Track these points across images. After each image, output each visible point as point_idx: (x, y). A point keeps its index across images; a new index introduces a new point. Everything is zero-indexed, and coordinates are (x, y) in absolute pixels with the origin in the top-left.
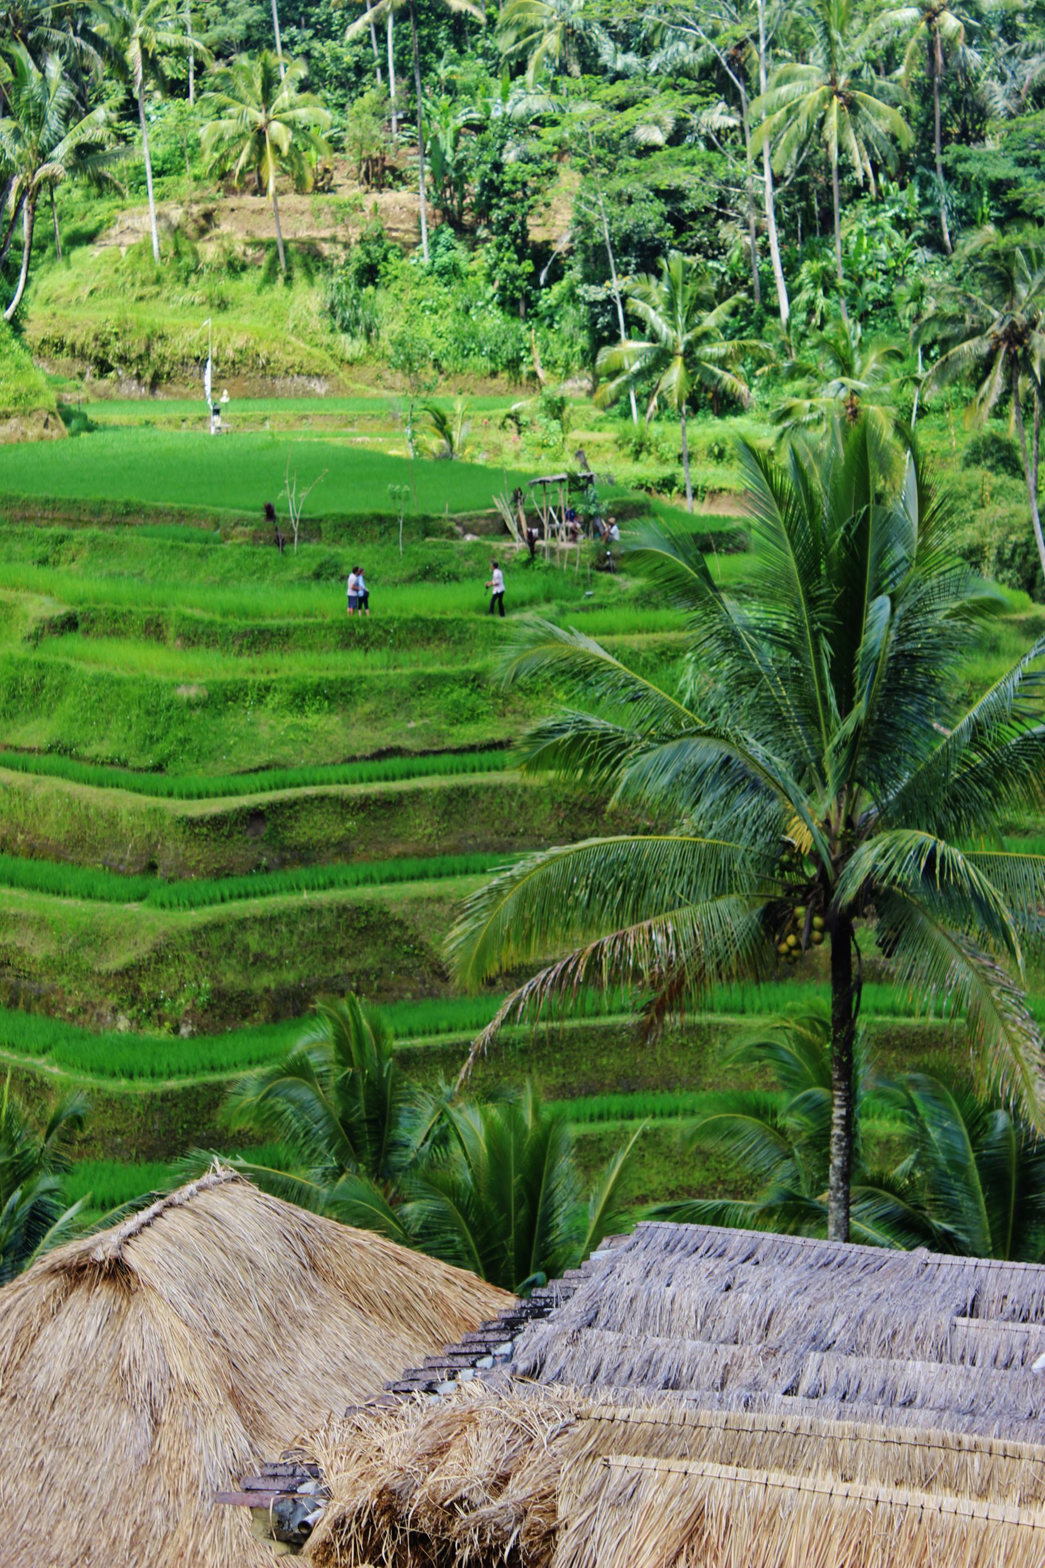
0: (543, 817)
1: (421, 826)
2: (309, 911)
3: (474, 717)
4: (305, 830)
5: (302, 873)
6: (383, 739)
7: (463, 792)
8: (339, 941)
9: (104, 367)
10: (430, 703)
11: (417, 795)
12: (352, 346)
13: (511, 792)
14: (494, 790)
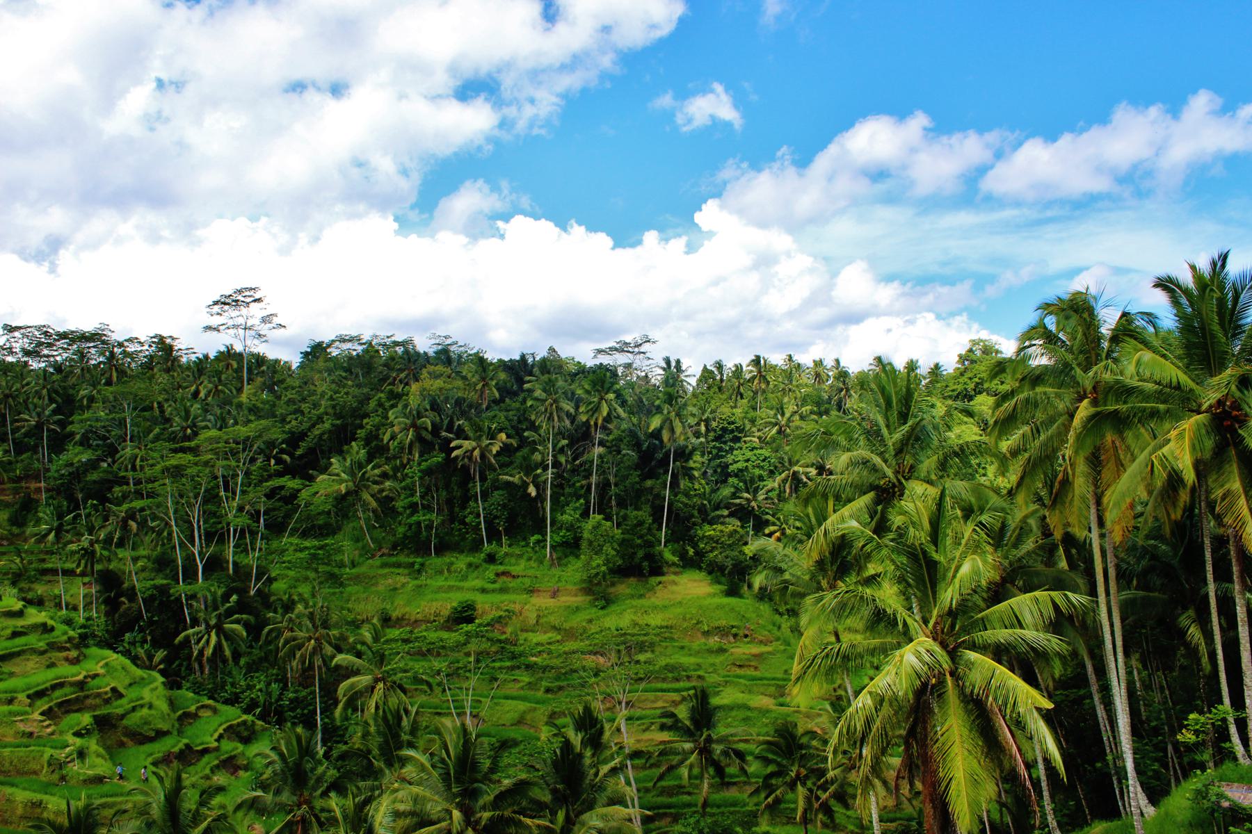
12: (15, 530)
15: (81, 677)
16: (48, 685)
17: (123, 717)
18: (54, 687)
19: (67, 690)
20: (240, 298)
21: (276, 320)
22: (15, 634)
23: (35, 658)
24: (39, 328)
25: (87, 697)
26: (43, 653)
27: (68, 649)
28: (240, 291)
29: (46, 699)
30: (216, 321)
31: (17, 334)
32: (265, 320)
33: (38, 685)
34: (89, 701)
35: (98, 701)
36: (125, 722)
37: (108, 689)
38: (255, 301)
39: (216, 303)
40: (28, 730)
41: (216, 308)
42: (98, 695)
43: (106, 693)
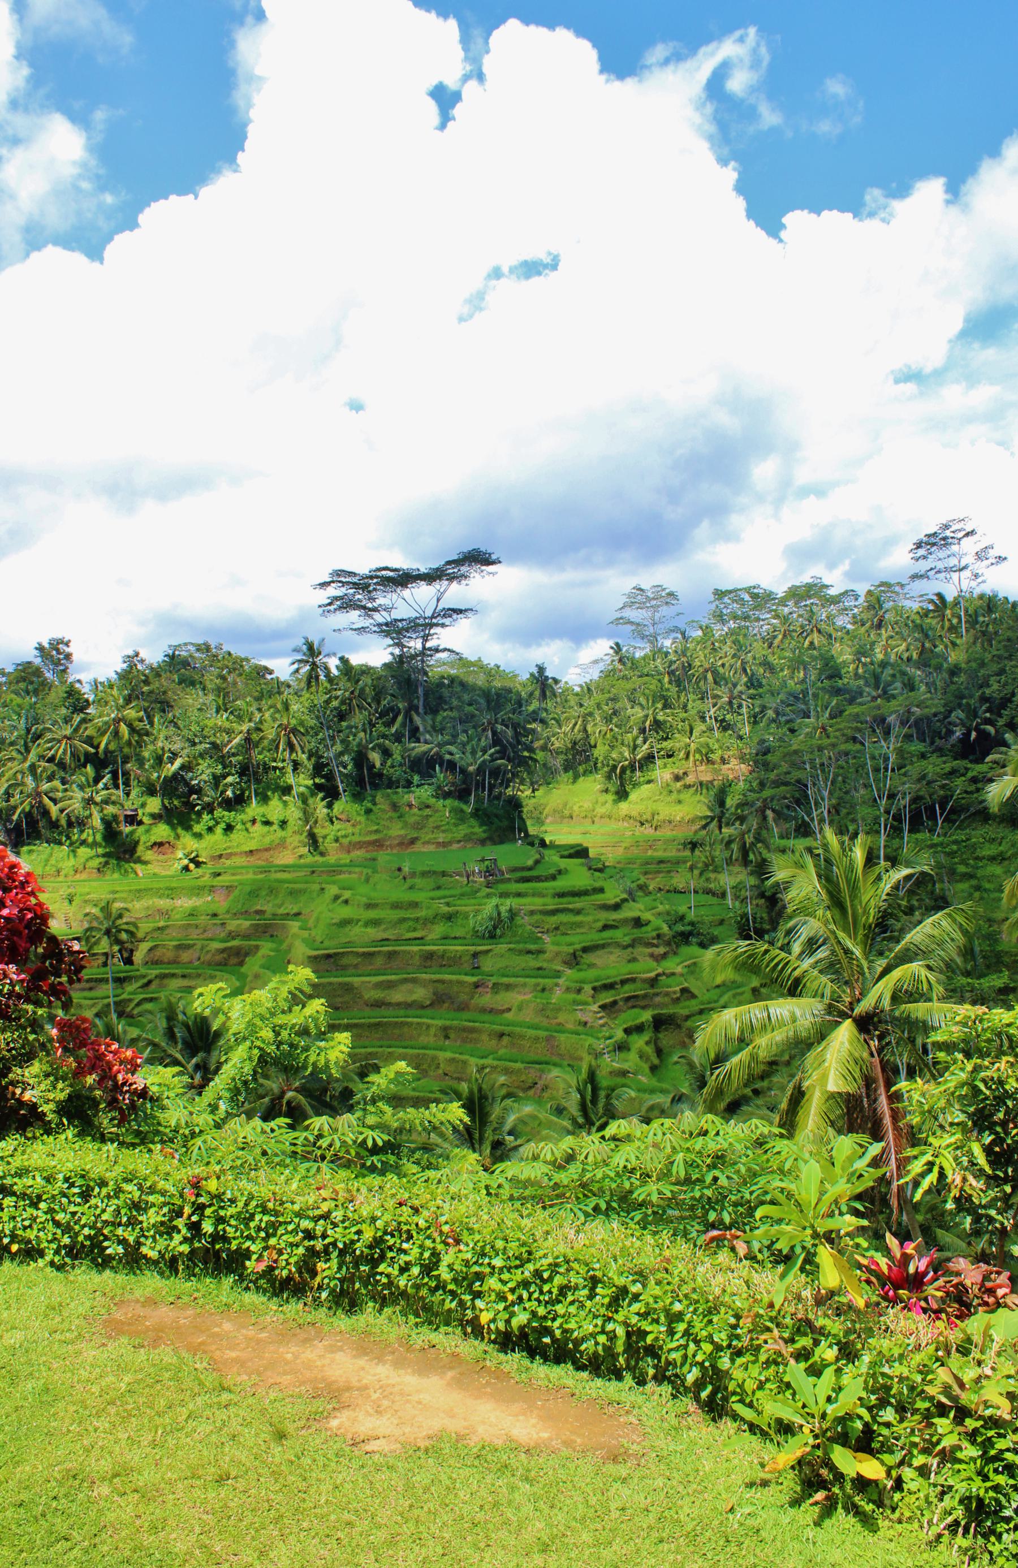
0: (417, 960)
1: (379, 961)
2: (330, 984)
3: (415, 930)
4: (345, 961)
5: (339, 973)
6: (385, 936)
7: (395, 952)
8: (339, 992)
9: (642, 824)
10: (406, 925)
11: (379, 952)
13: (409, 952)
14: (404, 952)
15: (653, 974)
16: (618, 979)
17: (687, 1017)
18: (623, 982)
19: (639, 985)
20: (948, 533)
21: (992, 553)
22: (606, 927)
23: (618, 952)
24: (748, 590)
25: (657, 994)
26: (626, 947)
27: (657, 946)
28: (946, 527)
29: (613, 992)
30: (923, 566)
31: (726, 600)
32: (979, 556)
33: (609, 977)
34: (657, 999)
35: (666, 999)
36: (689, 1023)
37: (678, 989)
38: (967, 535)
39: (919, 545)
40: (584, 1019)
41: (921, 552)
42: (667, 994)
43: (675, 993)
